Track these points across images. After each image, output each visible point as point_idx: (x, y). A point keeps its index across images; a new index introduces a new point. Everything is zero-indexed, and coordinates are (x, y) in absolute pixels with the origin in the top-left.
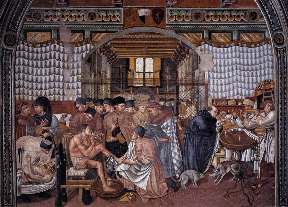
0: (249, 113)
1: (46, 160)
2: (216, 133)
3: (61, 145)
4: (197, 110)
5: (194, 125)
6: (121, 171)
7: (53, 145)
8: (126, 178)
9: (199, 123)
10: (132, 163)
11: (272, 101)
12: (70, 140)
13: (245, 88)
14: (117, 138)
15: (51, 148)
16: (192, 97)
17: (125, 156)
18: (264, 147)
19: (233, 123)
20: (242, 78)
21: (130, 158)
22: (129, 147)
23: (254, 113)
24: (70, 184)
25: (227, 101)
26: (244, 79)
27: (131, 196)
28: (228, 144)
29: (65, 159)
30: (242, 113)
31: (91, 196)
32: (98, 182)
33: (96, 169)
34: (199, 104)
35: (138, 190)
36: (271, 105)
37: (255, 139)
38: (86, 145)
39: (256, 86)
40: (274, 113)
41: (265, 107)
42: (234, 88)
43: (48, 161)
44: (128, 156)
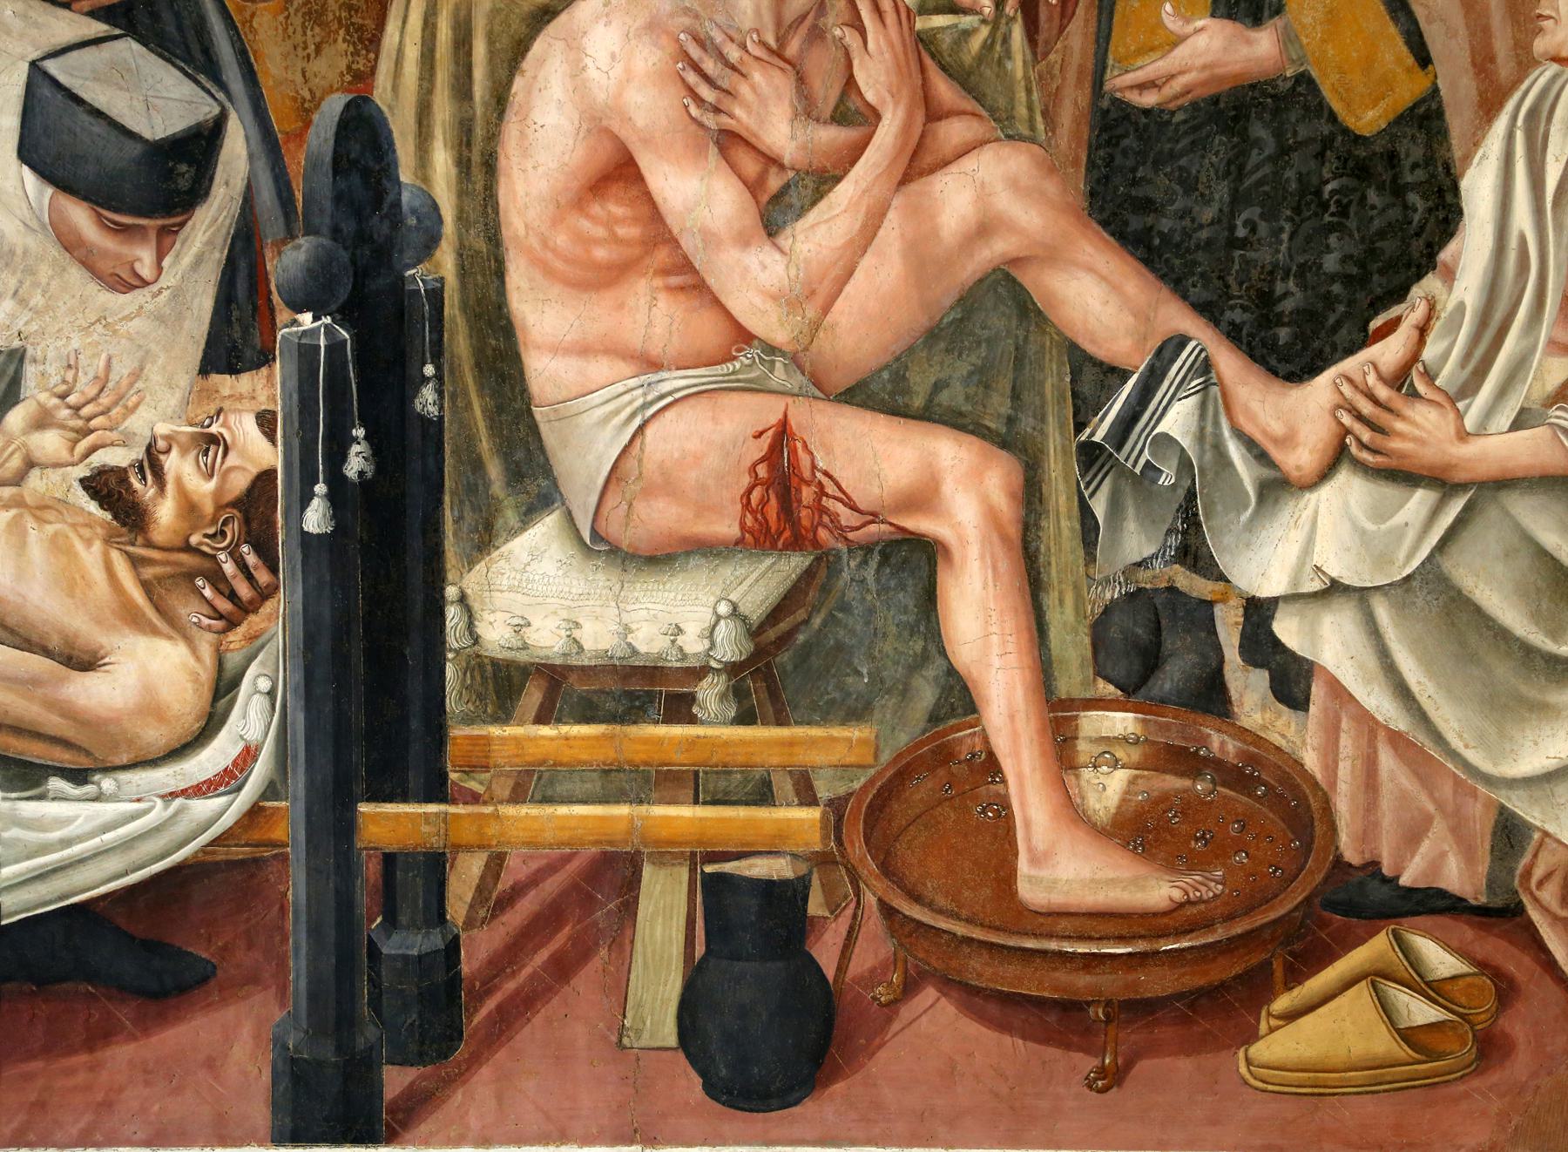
1: (113, 397)
3: (363, 136)
6: (1316, 586)
7: (236, 152)
8: (1378, 702)
10: (1484, 471)
12: (513, 54)
14: (1288, 39)
15: (197, 194)
17: (1389, 352)
21: (1470, 388)
22: (1478, 188)
24: (503, 789)
27: (1433, 990)
29: (428, 394)
31: (830, 973)
32: (944, 755)
33: (915, 560)
35: (1549, 895)
38: (772, 161)
43: (159, 412)
44: (1445, 354)
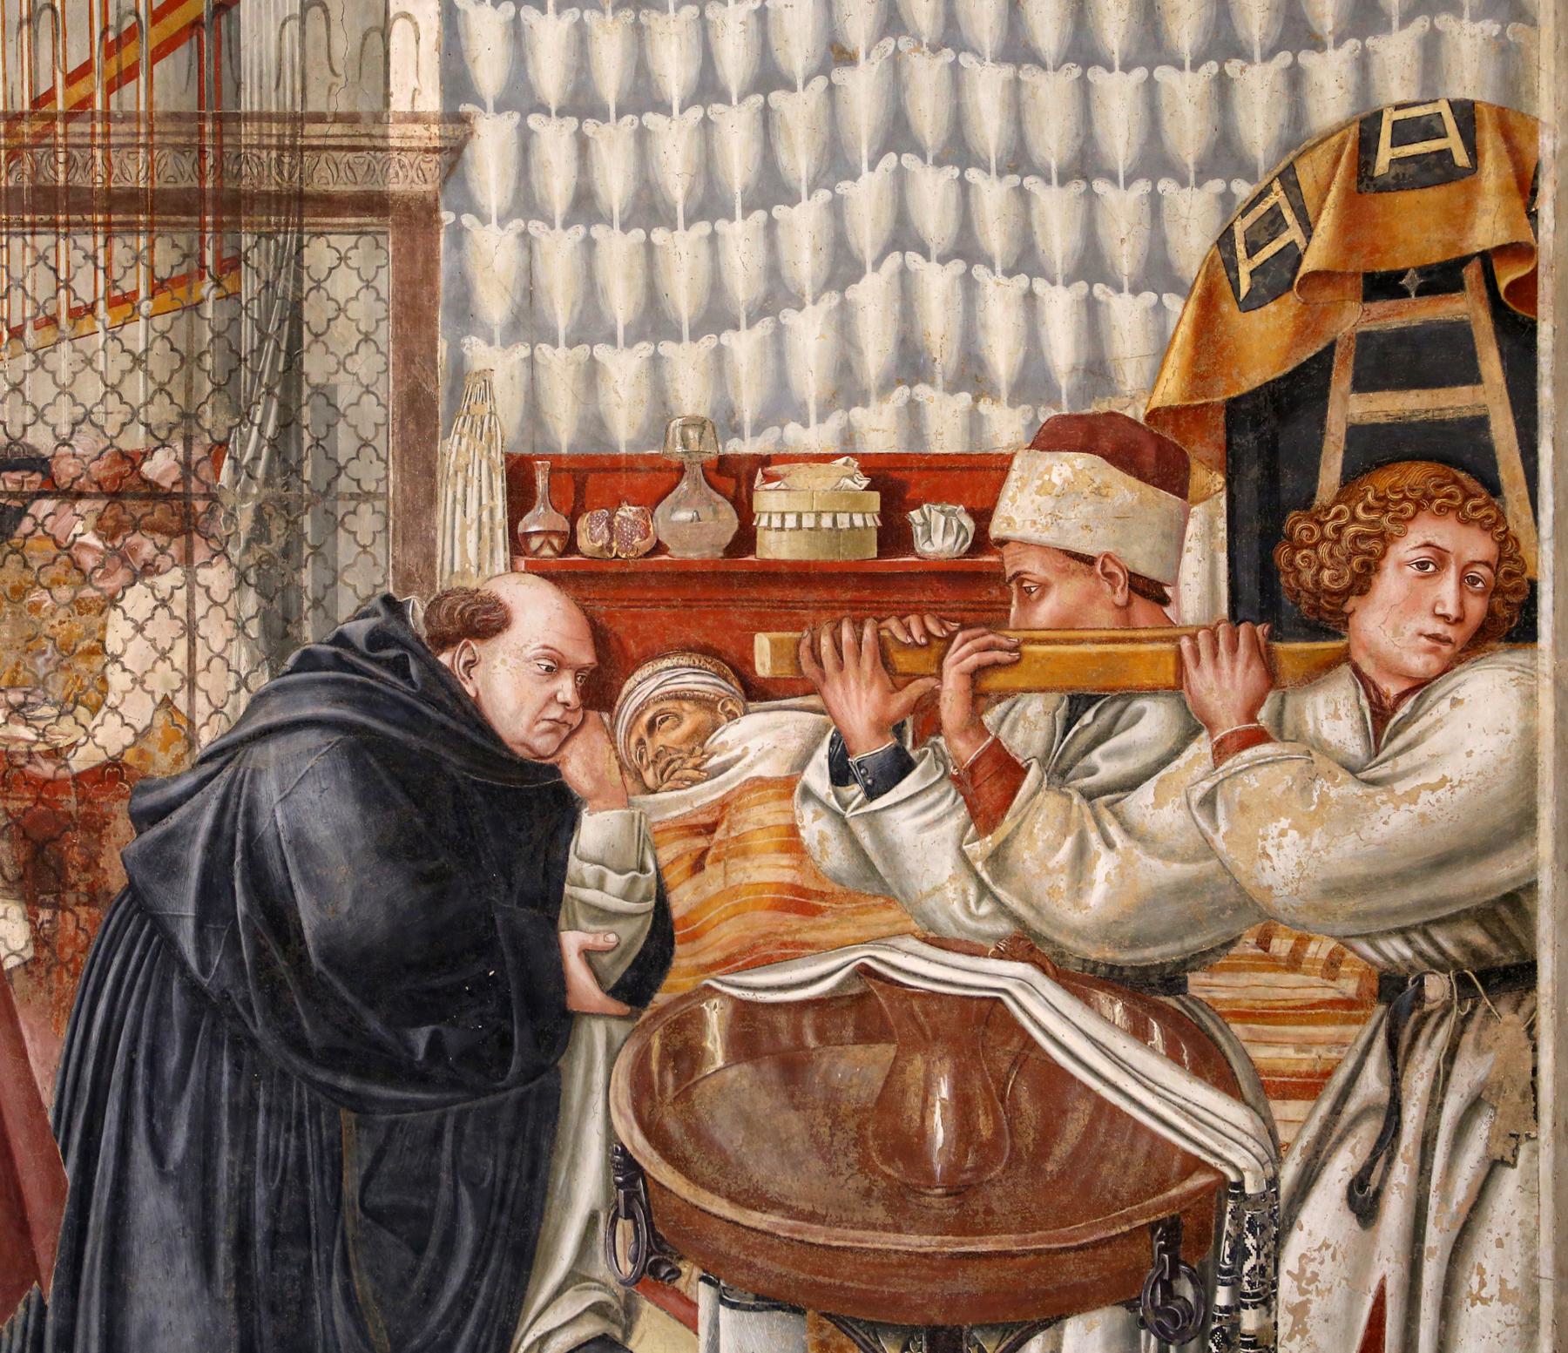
0: (1088, 686)
2: (555, 1023)
4: (278, 632)
5: (212, 893)
9: (301, 843)
11: (1495, 489)
13: (1027, 260)
16: (189, 416)
18: (1352, 1298)
19: (834, 858)
20: (987, 86)
23: (1176, 688)
25: (735, 479)
26: (1017, 107)
28: (756, 1219)
30: (978, 694)
34: (293, 524)
36: (1477, 546)
37: (1187, 1136)
39: (1214, 227)
40: (1530, 699)
41: (1362, 583)
42: (843, 267)
